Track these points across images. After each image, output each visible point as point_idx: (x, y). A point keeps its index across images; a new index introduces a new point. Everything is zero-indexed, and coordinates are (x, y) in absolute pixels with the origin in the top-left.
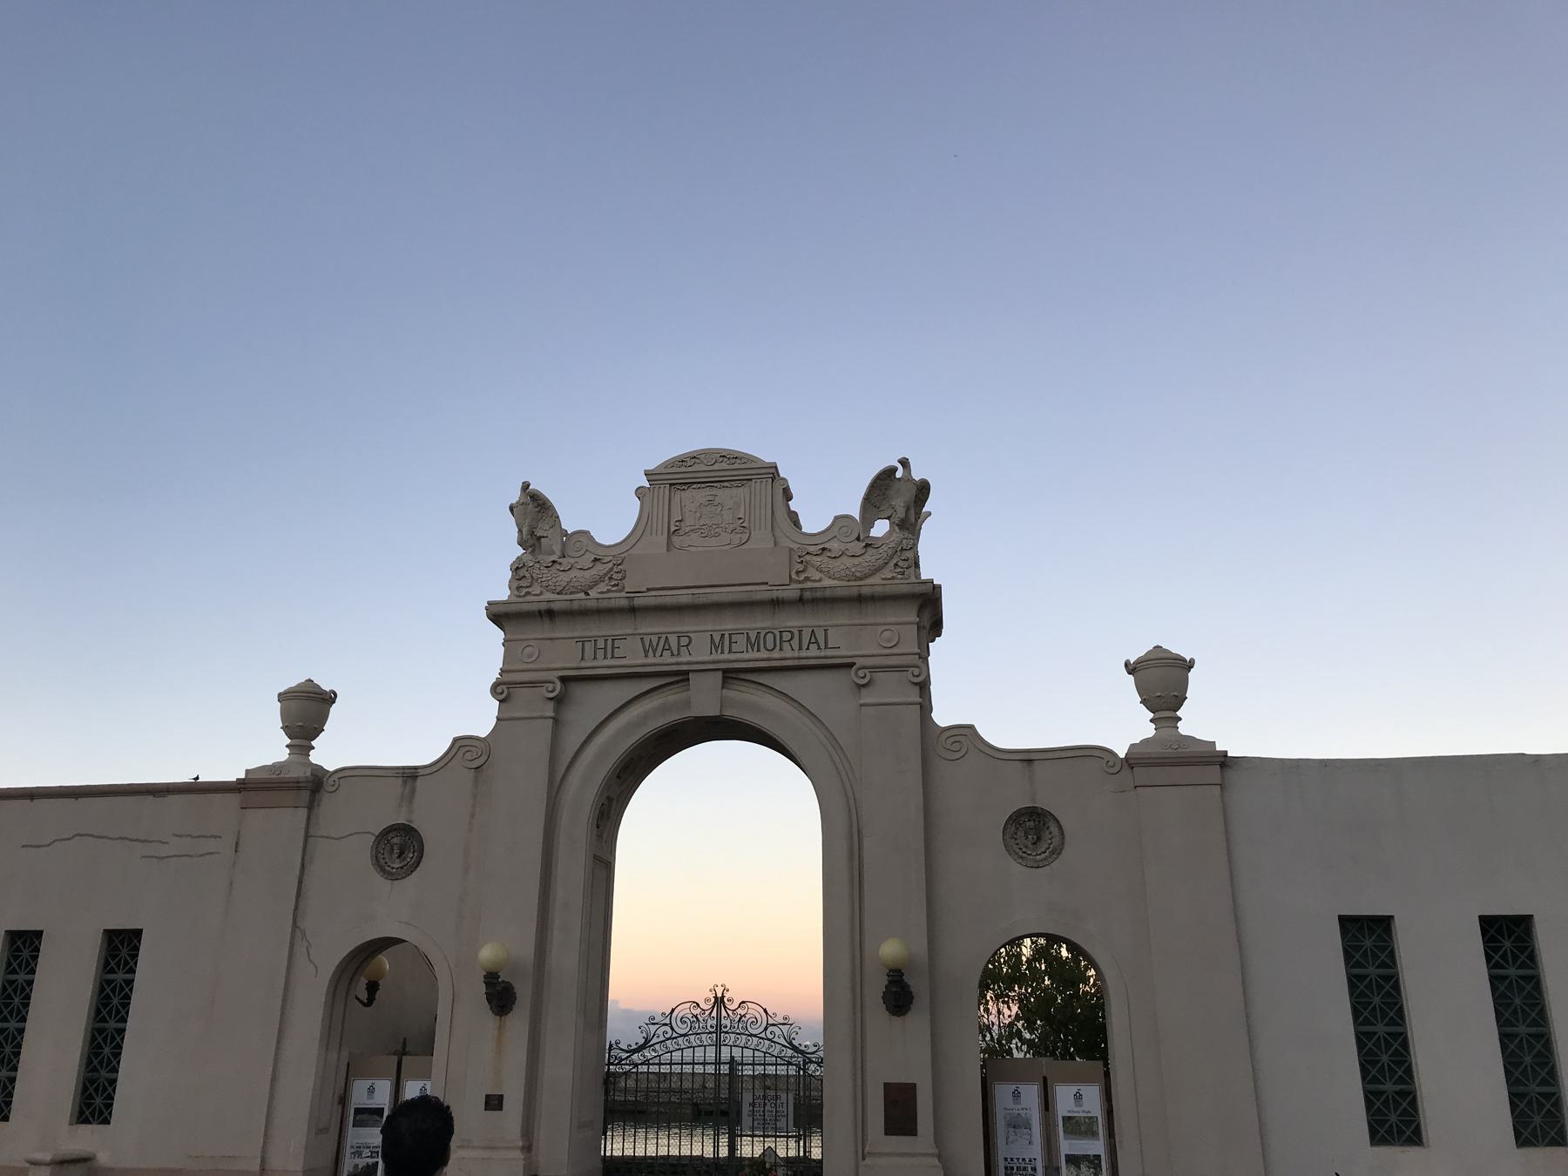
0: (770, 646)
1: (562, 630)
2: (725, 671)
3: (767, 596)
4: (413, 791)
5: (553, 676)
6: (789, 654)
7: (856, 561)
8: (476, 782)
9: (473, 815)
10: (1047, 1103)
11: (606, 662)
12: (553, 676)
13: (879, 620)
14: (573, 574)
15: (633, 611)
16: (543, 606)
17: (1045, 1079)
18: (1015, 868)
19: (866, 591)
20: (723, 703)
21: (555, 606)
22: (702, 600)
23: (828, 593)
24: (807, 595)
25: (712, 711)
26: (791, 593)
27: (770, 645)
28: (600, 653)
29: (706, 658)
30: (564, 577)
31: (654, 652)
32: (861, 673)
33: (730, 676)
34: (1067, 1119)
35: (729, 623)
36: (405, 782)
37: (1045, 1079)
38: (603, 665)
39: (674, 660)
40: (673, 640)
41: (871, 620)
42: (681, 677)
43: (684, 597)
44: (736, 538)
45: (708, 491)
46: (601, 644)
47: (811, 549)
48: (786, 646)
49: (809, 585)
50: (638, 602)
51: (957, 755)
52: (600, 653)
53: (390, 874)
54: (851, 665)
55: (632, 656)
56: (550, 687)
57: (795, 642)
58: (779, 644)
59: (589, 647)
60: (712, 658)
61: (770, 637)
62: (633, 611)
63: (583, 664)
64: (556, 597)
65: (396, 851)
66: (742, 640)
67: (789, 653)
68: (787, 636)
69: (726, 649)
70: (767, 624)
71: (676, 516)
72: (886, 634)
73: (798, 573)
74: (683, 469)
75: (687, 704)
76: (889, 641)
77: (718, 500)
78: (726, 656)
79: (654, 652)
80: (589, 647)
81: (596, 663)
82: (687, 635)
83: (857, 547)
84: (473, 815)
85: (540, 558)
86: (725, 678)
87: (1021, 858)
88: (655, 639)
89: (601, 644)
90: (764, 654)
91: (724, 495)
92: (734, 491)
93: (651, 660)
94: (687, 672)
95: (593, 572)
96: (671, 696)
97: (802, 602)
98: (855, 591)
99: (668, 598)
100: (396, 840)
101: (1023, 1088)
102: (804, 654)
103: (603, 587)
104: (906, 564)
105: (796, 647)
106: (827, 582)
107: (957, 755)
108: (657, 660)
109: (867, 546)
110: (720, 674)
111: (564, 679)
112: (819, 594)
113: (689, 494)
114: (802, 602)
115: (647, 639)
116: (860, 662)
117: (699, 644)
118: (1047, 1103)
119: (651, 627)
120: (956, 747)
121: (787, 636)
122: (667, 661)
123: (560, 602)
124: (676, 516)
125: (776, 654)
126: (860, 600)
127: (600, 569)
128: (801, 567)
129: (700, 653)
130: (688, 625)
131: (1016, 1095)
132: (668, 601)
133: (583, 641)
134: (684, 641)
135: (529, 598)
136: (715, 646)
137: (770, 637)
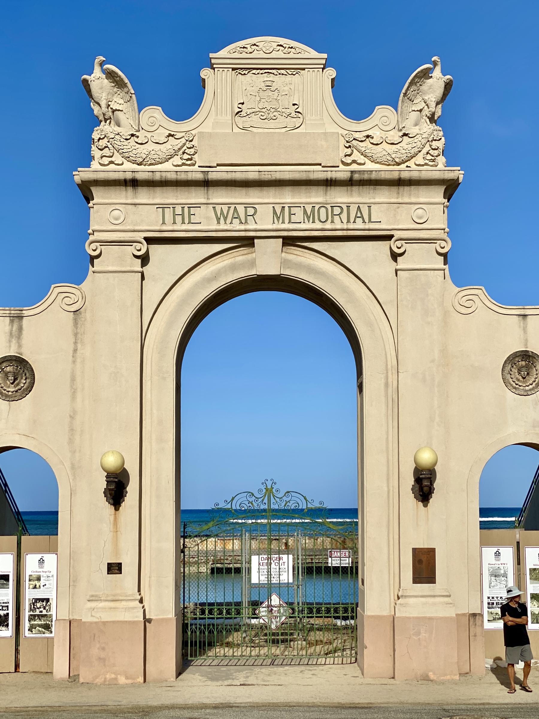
0: (323, 218)
1: (144, 196)
2: (284, 238)
3: (322, 176)
4: (20, 329)
5: (140, 236)
6: (339, 226)
8: (76, 322)
9: (75, 351)
10: (519, 560)
11: (184, 227)
12: (140, 236)
13: (413, 200)
14: (150, 146)
15: (206, 184)
16: (129, 176)
17: (518, 543)
18: (510, 395)
19: (405, 175)
20: (285, 263)
21: (140, 176)
22: (266, 177)
23: (374, 176)
24: (356, 177)
25: (273, 270)
26: (342, 173)
27: (323, 218)
29: (270, 227)
30: (143, 150)
31: (225, 219)
32: (399, 243)
33: (289, 241)
34: (533, 570)
35: (288, 197)
36: (12, 322)
37: (518, 543)
38: (182, 229)
39: (243, 227)
40: (241, 209)
41: (406, 200)
42: (248, 242)
43: (252, 173)
44: (292, 122)
45: (266, 77)
46: (179, 210)
47: (357, 135)
48: (336, 218)
49: (354, 167)
50: (213, 176)
51: (470, 310)
52: (179, 219)
53: (7, 396)
54: (389, 238)
55: (206, 222)
56: (138, 246)
57: (344, 216)
60: (275, 227)
61: (323, 210)
62: (206, 184)
63: (164, 228)
64: (135, 167)
65: (11, 378)
67: (338, 225)
69: (287, 220)
70: (320, 199)
72: (420, 212)
74: (244, 55)
75: (253, 263)
76: (420, 218)
77: (274, 86)
79: (225, 219)
80: (168, 213)
81: (176, 227)
82: (252, 205)
83: (395, 136)
84: (75, 351)
86: (284, 244)
87: (514, 389)
88: (225, 208)
89: (179, 210)
91: (279, 81)
93: (222, 226)
94: (253, 238)
95: (168, 146)
96: (240, 256)
97: (350, 183)
98: (395, 175)
99: (239, 174)
100: (8, 369)
101: (502, 550)
102: (351, 226)
103: (177, 160)
104: (436, 153)
105: (345, 221)
106: (370, 166)
107: (470, 310)
109: (405, 135)
110: (281, 240)
112: (366, 176)
114: (350, 183)
115: (218, 208)
117: (263, 213)
118: (519, 560)
119: (220, 197)
122: (236, 228)
123: (143, 173)
125: (328, 226)
126: (399, 183)
128: (349, 151)
129: (264, 222)
130: (253, 196)
131: (498, 554)
132: (238, 176)
133: (163, 207)
134: (251, 211)
135: (112, 166)
137: (323, 210)
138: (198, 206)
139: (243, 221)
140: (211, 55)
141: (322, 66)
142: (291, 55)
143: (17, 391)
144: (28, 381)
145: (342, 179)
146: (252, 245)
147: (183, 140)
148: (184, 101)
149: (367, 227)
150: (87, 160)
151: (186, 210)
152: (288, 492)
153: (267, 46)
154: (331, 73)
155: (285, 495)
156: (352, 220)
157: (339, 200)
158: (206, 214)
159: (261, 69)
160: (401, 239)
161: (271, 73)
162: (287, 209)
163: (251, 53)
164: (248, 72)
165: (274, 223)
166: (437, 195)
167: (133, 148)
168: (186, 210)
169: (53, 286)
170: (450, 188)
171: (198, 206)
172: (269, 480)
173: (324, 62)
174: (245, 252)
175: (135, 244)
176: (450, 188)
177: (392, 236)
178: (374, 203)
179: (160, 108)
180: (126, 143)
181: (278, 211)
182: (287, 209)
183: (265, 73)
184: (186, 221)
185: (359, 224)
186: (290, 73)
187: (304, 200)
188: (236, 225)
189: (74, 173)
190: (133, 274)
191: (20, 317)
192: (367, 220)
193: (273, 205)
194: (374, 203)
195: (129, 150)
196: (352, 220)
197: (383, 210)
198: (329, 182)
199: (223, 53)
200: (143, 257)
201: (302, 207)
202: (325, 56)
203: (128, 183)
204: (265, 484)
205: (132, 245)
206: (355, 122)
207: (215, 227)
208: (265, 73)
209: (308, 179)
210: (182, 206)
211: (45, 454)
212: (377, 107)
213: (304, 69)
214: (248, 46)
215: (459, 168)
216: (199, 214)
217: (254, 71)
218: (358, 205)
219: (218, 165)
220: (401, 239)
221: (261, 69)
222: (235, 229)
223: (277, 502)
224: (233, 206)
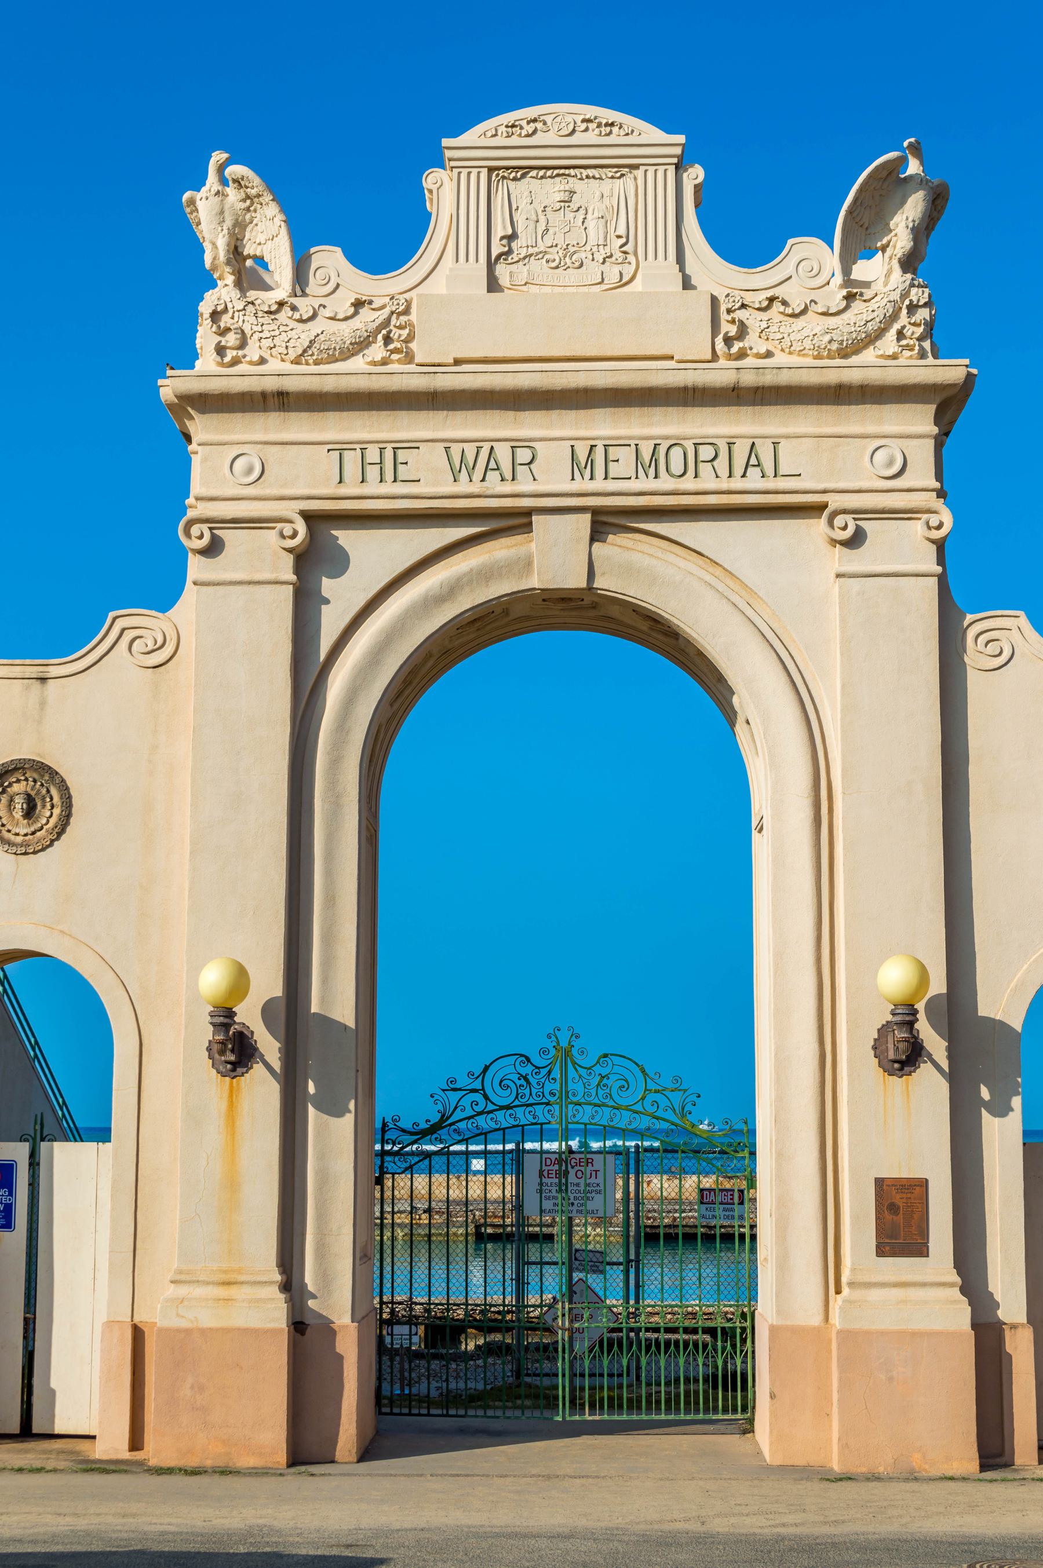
0: (677, 467)
1: (300, 426)
2: (596, 512)
4: (43, 704)
6: (712, 484)
7: (832, 321)
12: (290, 509)
13: (871, 429)
28: (373, 472)
36: (28, 688)
38: (379, 492)
39: (507, 488)
40: (503, 452)
42: (515, 521)
46: (373, 455)
47: (748, 298)
48: (705, 469)
52: (373, 472)
55: (431, 480)
58: (693, 466)
59: (352, 459)
61: (676, 454)
66: (626, 455)
67: (710, 483)
68: (706, 452)
71: (500, 229)
73: (728, 341)
74: (515, 141)
75: (526, 565)
78: (599, 484)
80: (352, 459)
82: (527, 443)
85: (252, 295)
88: (470, 450)
89: (373, 455)
90: (666, 483)
92: (607, 186)
93: (464, 486)
94: (529, 513)
102: (737, 484)
105: (724, 472)
108: (475, 488)
110: (588, 517)
111: (308, 517)
113: (522, 189)
115: (456, 450)
116: (835, 502)
117: (548, 458)
120: (992, 649)
121: (706, 452)
124: (500, 229)
125: (688, 483)
127: (367, 319)
129: (552, 476)
130: (529, 425)
133: (340, 449)
134: (523, 455)
136: (580, 465)
137: (676, 454)
138: (413, 445)
139: (508, 475)
140: (446, 142)
141: (675, 160)
142: (612, 140)
143: (33, 833)
144: (57, 811)
145: (718, 385)
146: (528, 527)
147: (386, 312)
148: (389, 237)
149: (771, 484)
150: (188, 357)
151: (389, 454)
152: (606, 1056)
153: (561, 122)
154: (696, 174)
155: (598, 1062)
156: (738, 470)
157: (712, 430)
158: (430, 459)
159: (547, 168)
160: (845, 512)
161: (569, 175)
162: (599, 452)
163: (528, 136)
164: (523, 176)
165: (573, 479)
166: (921, 420)
167: (282, 328)
168: (389, 454)
169: (112, 615)
170: (949, 404)
171: (413, 445)
172: (564, 1029)
173: (678, 151)
174: (514, 542)
175: (279, 525)
176: (949, 404)
177: (824, 506)
178: (787, 437)
179: (338, 250)
180: (267, 319)
181: (582, 455)
182: (599, 452)
183: (558, 175)
184: (389, 475)
185: (754, 480)
186: (610, 175)
187: (636, 431)
188: (494, 484)
189: (160, 382)
190: (277, 586)
191: (43, 680)
192: (770, 470)
193: (572, 443)
194: (787, 437)
195: (273, 333)
196: (738, 470)
197: (809, 450)
198: (691, 393)
199: (471, 137)
200: (299, 551)
201: (633, 447)
202: (681, 139)
203: (271, 402)
204: (553, 1038)
205: (274, 528)
206: (746, 270)
207: (450, 489)
208: (558, 175)
209: (646, 385)
210: (382, 445)
211: (87, 967)
212: (790, 242)
213: (636, 167)
214: (524, 123)
215: (967, 361)
216: (415, 463)
217: (534, 173)
218: (751, 441)
219: (457, 362)
220: (845, 512)
221: (547, 168)
222: (489, 492)
223: (580, 1076)
224: (486, 447)
